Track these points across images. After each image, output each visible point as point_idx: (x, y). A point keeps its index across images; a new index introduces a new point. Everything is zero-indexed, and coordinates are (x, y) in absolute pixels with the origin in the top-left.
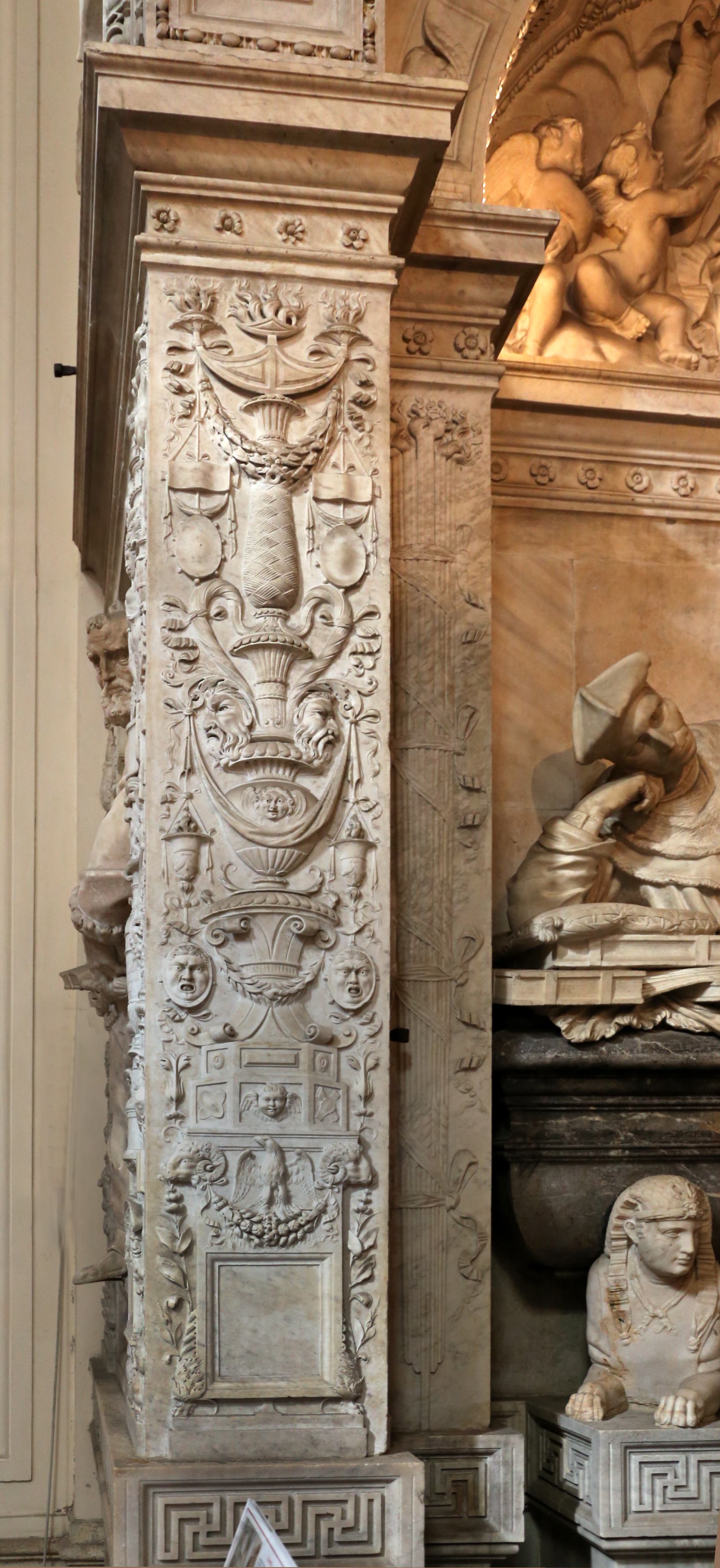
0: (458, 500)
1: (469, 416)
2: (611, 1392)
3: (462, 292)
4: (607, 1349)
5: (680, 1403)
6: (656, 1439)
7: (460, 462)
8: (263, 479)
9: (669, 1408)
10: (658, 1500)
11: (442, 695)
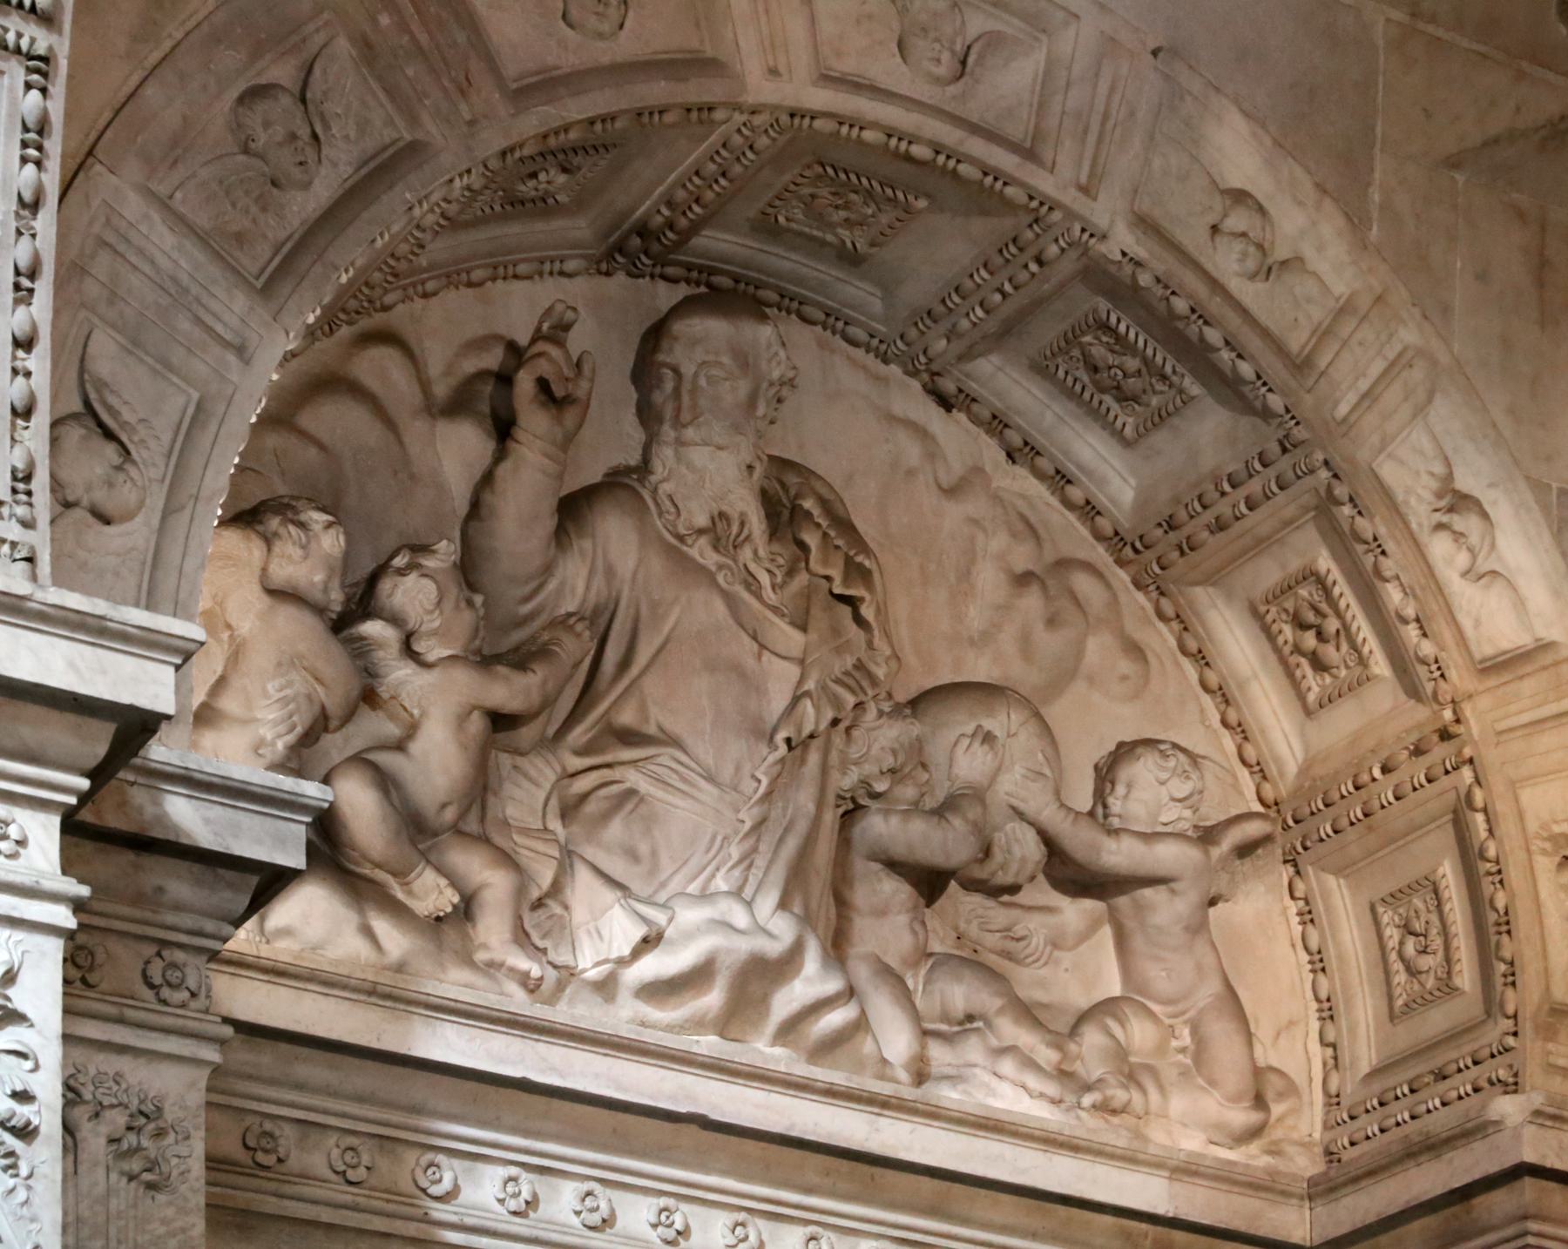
7: (151, 1186)
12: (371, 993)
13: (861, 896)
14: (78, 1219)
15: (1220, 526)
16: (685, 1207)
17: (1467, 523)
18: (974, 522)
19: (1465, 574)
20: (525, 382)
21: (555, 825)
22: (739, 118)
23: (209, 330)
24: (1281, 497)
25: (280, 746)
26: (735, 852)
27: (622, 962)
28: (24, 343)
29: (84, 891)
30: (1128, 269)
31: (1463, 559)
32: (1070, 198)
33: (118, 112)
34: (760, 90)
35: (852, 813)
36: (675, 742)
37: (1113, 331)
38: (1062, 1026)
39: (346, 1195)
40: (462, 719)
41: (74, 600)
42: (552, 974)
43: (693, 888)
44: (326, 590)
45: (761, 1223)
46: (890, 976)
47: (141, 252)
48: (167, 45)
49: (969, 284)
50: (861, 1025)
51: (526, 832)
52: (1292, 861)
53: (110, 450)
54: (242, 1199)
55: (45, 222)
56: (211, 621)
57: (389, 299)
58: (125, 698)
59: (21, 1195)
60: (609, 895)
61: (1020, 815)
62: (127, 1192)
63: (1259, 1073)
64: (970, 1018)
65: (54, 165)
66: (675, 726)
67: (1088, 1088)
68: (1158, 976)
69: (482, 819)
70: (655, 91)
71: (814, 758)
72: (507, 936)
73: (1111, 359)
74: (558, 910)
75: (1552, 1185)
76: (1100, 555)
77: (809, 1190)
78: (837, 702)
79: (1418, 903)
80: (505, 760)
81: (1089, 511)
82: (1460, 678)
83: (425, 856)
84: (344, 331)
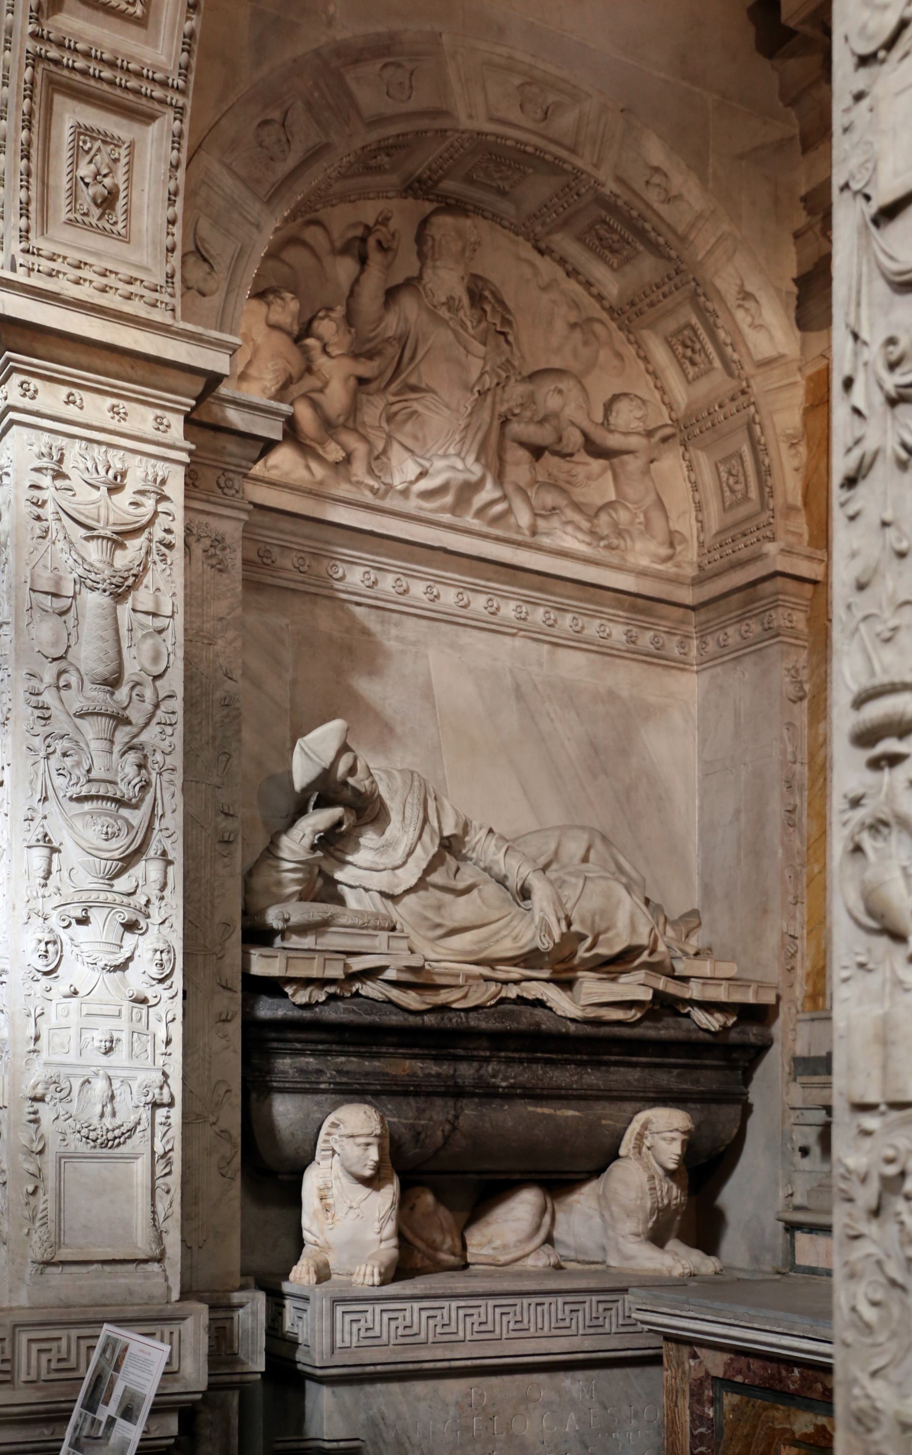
0: (219, 599)
1: (227, 537)
3: (224, 448)
7: (220, 570)
8: (97, 592)
11: (207, 743)
12: (310, 493)
13: (509, 457)
14: (191, 583)
15: (652, 305)
16: (438, 586)
17: (750, 304)
18: (554, 302)
19: (750, 326)
20: (372, 242)
21: (384, 425)
22: (457, 135)
23: (245, 218)
24: (676, 293)
25: (273, 389)
26: (457, 437)
27: (412, 483)
28: (172, 222)
29: (193, 447)
30: (613, 198)
31: (749, 319)
32: (589, 169)
33: (210, 131)
34: (465, 123)
35: (505, 422)
36: (434, 392)
37: (608, 224)
38: (592, 512)
39: (300, 577)
40: (347, 379)
41: (190, 327)
42: (383, 487)
43: (441, 452)
44: (292, 325)
45: (469, 593)
46: (522, 491)
47: (219, 186)
48: (230, 104)
49: (549, 204)
50: (509, 511)
51: (372, 427)
52: (684, 444)
53: (206, 267)
54: (258, 577)
55: (181, 174)
56: (246, 337)
57: (318, 206)
58: (209, 368)
59: (168, 572)
60: (406, 455)
61: (573, 424)
62: (210, 572)
63: (671, 532)
64: (554, 508)
65: (184, 150)
66: (433, 385)
67: (602, 538)
68: (631, 492)
69: (355, 422)
70: (424, 124)
71: (489, 399)
72: (364, 470)
73: (607, 235)
74: (385, 460)
75: (788, 580)
76: (604, 316)
77: (488, 580)
78: (499, 376)
79: (734, 462)
80: (364, 397)
81: (600, 298)
82: (749, 369)
83: (331, 436)
84: (300, 220)
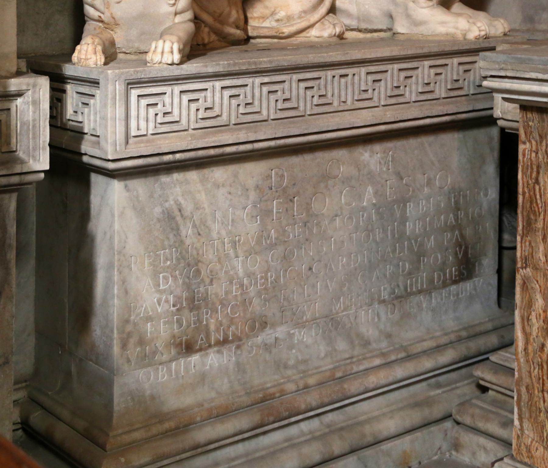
2: (107, 43)
4: (102, 8)
5: (168, 45)
6: (152, 75)
9: (159, 50)
10: (151, 125)
